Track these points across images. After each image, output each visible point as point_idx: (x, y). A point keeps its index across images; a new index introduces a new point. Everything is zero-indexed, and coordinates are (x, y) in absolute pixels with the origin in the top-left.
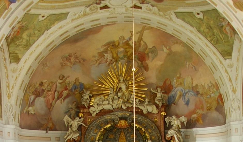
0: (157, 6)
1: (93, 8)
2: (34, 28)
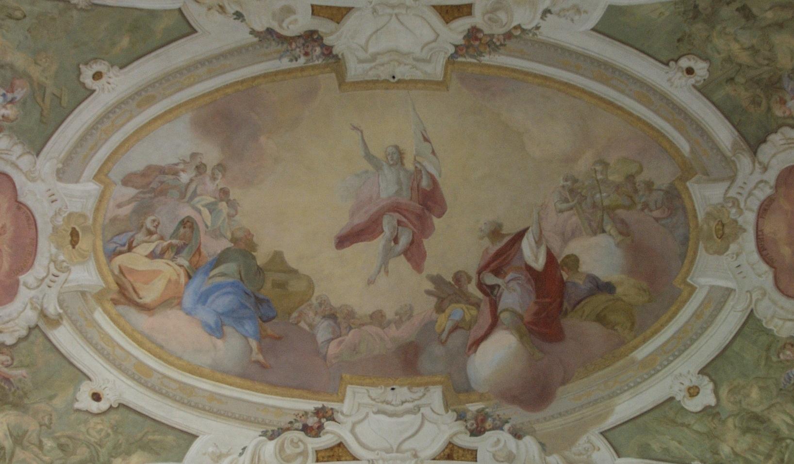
0: (533, 433)
1: (289, 450)
2: (46, 421)
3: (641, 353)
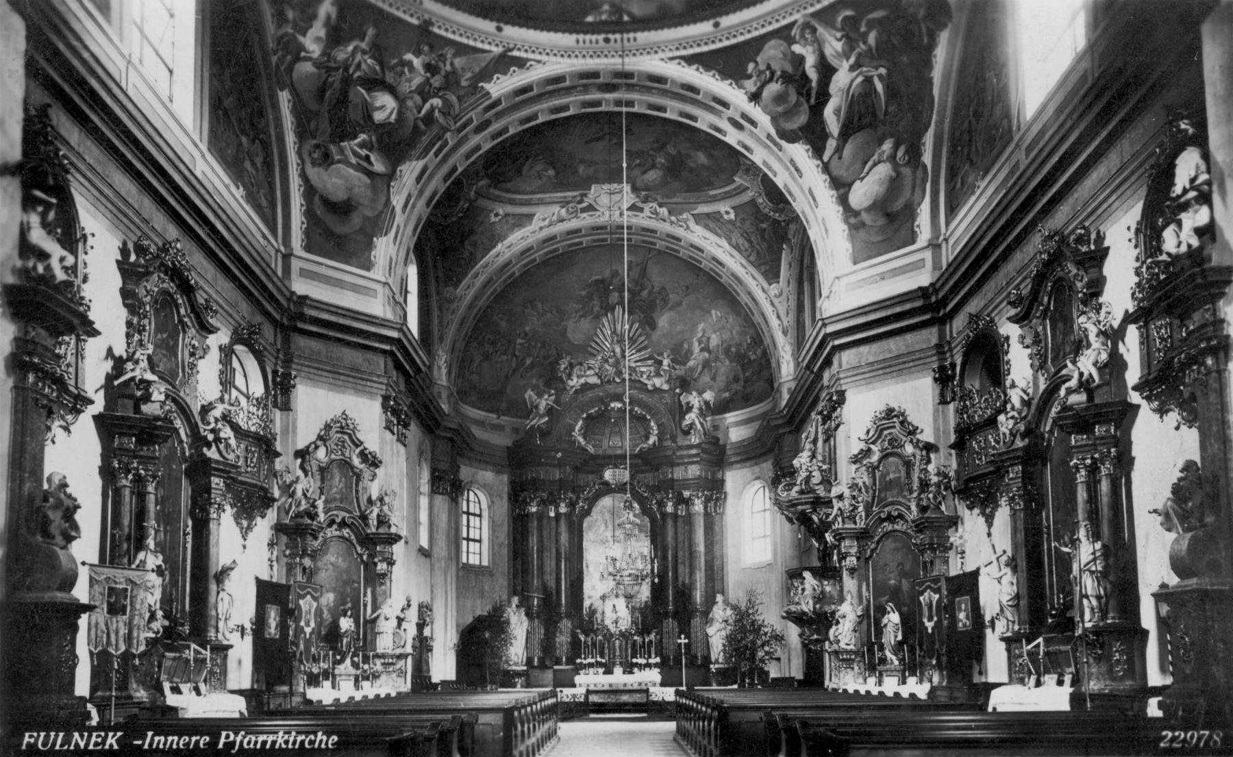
3: (712, 193)
